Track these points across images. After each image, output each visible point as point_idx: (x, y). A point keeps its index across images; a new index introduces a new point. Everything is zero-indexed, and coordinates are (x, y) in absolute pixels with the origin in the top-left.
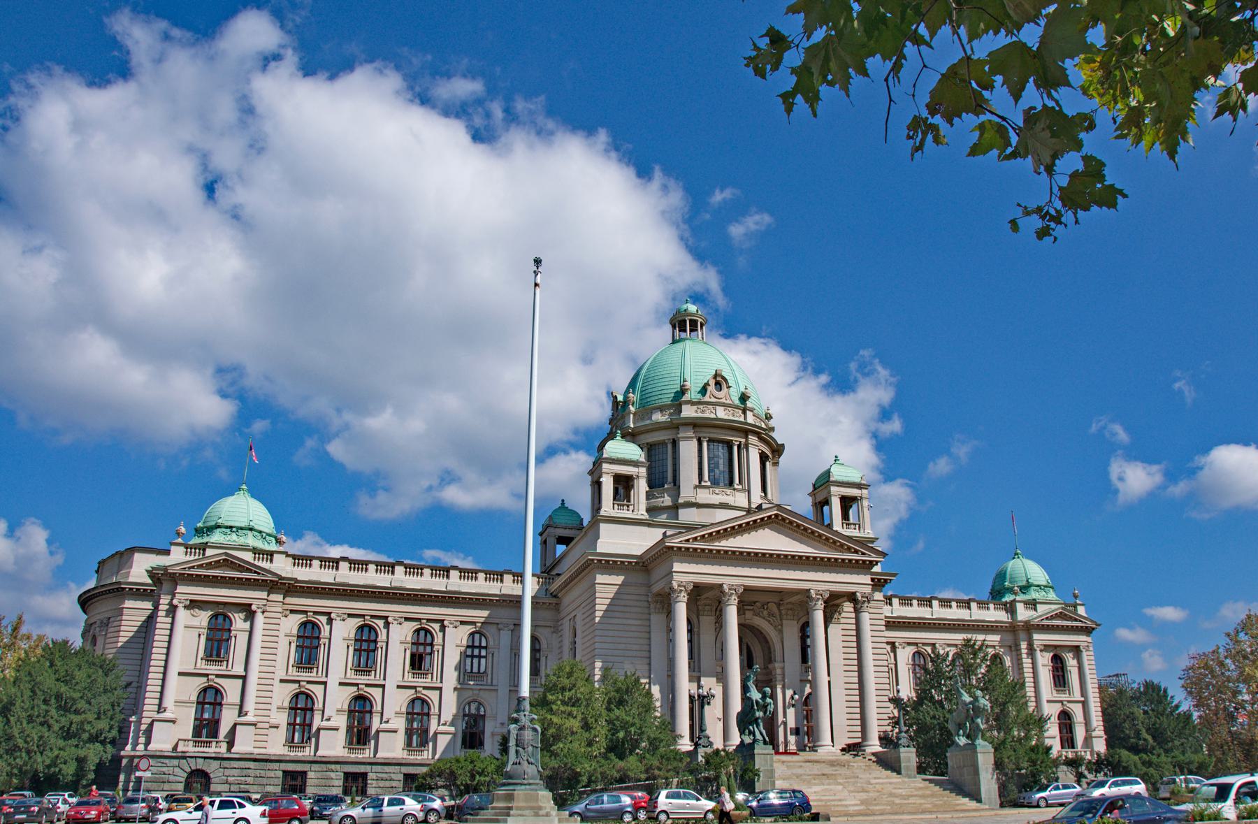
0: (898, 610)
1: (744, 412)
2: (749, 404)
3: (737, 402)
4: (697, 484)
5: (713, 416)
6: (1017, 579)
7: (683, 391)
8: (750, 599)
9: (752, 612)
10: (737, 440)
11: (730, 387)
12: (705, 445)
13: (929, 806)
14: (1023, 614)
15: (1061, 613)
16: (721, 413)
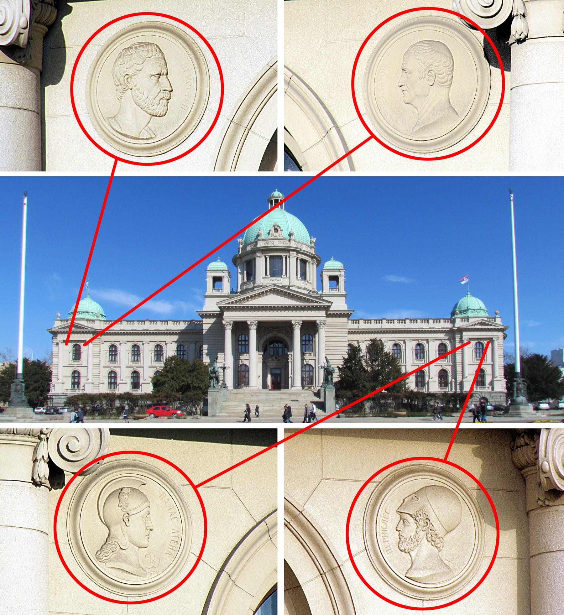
0: (355, 326)
1: (289, 241)
2: (292, 237)
3: (287, 237)
4: (264, 276)
5: (272, 245)
6: (462, 307)
7: (258, 235)
8: (262, 326)
9: (276, 332)
10: (284, 254)
11: (282, 230)
12: (268, 259)
13: (296, 413)
14: (459, 323)
15: (481, 322)
16: (276, 243)
